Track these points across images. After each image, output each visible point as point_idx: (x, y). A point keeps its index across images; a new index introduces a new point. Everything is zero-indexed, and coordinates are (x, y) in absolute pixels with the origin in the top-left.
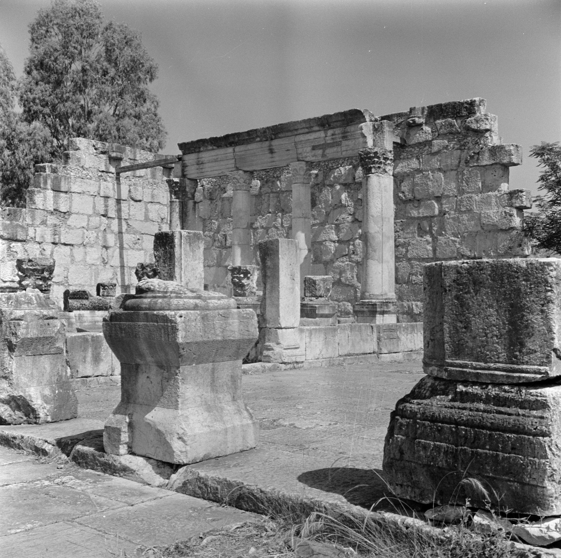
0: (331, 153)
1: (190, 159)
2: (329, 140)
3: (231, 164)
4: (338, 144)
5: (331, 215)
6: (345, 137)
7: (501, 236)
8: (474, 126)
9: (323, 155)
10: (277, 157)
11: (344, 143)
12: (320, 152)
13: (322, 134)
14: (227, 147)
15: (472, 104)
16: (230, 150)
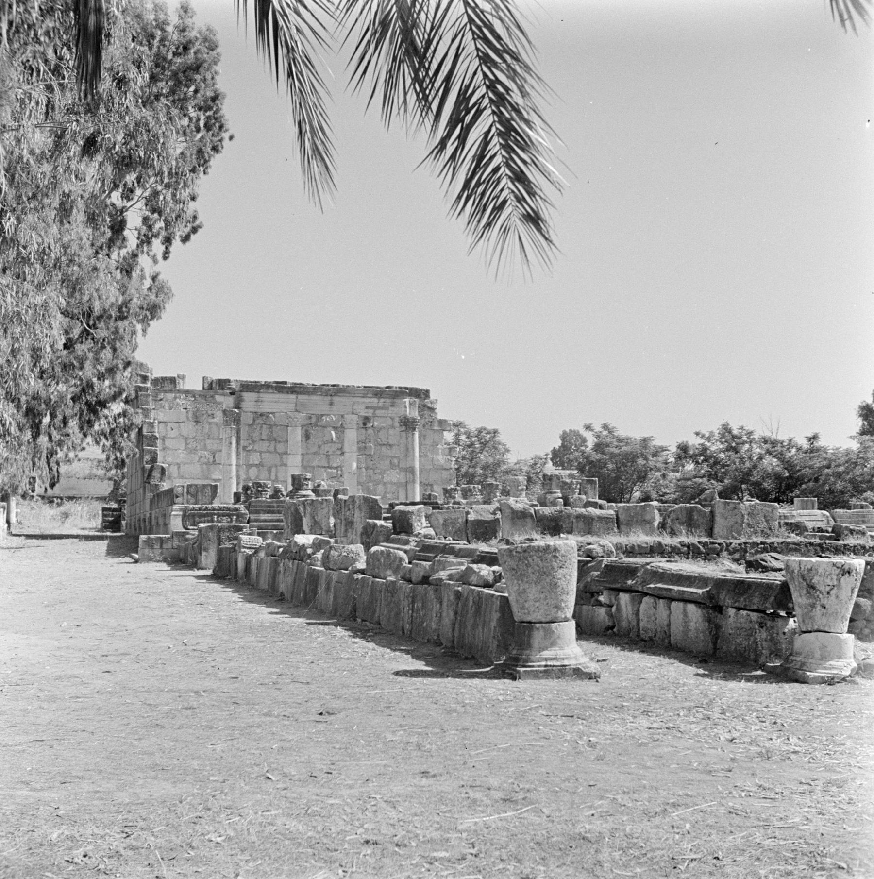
0: (378, 412)
1: (249, 397)
2: (381, 405)
3: (292, 406)
4: (387, 408)
5: (323, 447)
6: (392, 406)
7: (444, 472)
8: (430, 405)
9: (374, 413)
10: (334, 408)
11: (391, 409)
12: (372, 411)
13: (375, 400)
14: (288, 393)
15: (427, 391)
16: (293, 396)
